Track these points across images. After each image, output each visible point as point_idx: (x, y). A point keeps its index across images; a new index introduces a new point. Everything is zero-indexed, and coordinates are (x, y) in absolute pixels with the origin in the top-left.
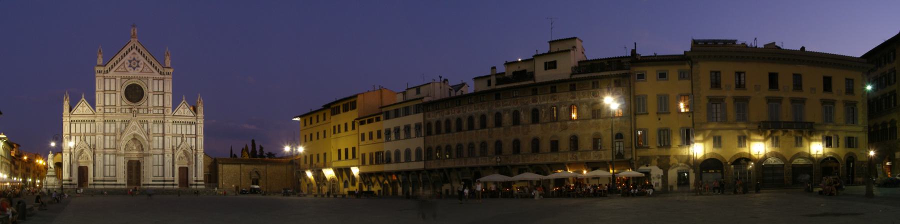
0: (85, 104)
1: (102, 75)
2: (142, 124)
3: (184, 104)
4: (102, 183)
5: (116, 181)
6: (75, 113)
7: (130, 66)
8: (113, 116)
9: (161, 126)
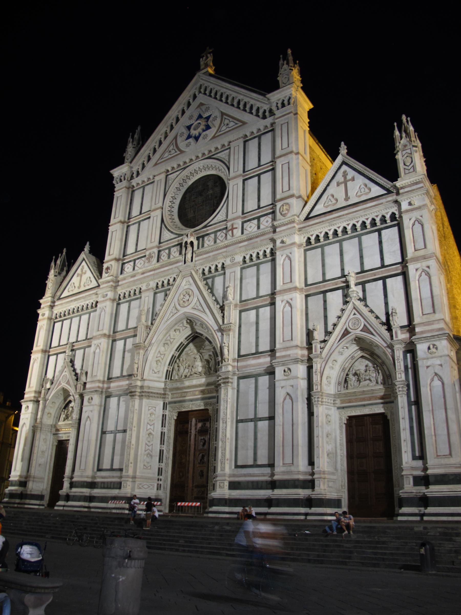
0: (86, 267)
1: (125, 183)
2: (210, 281)
3: (344, 168)
4: (86, 491)
5: (119, 486)
6: (65, 294)
7: (189, 137)
8: (136, 278)
9: (266, 268)
